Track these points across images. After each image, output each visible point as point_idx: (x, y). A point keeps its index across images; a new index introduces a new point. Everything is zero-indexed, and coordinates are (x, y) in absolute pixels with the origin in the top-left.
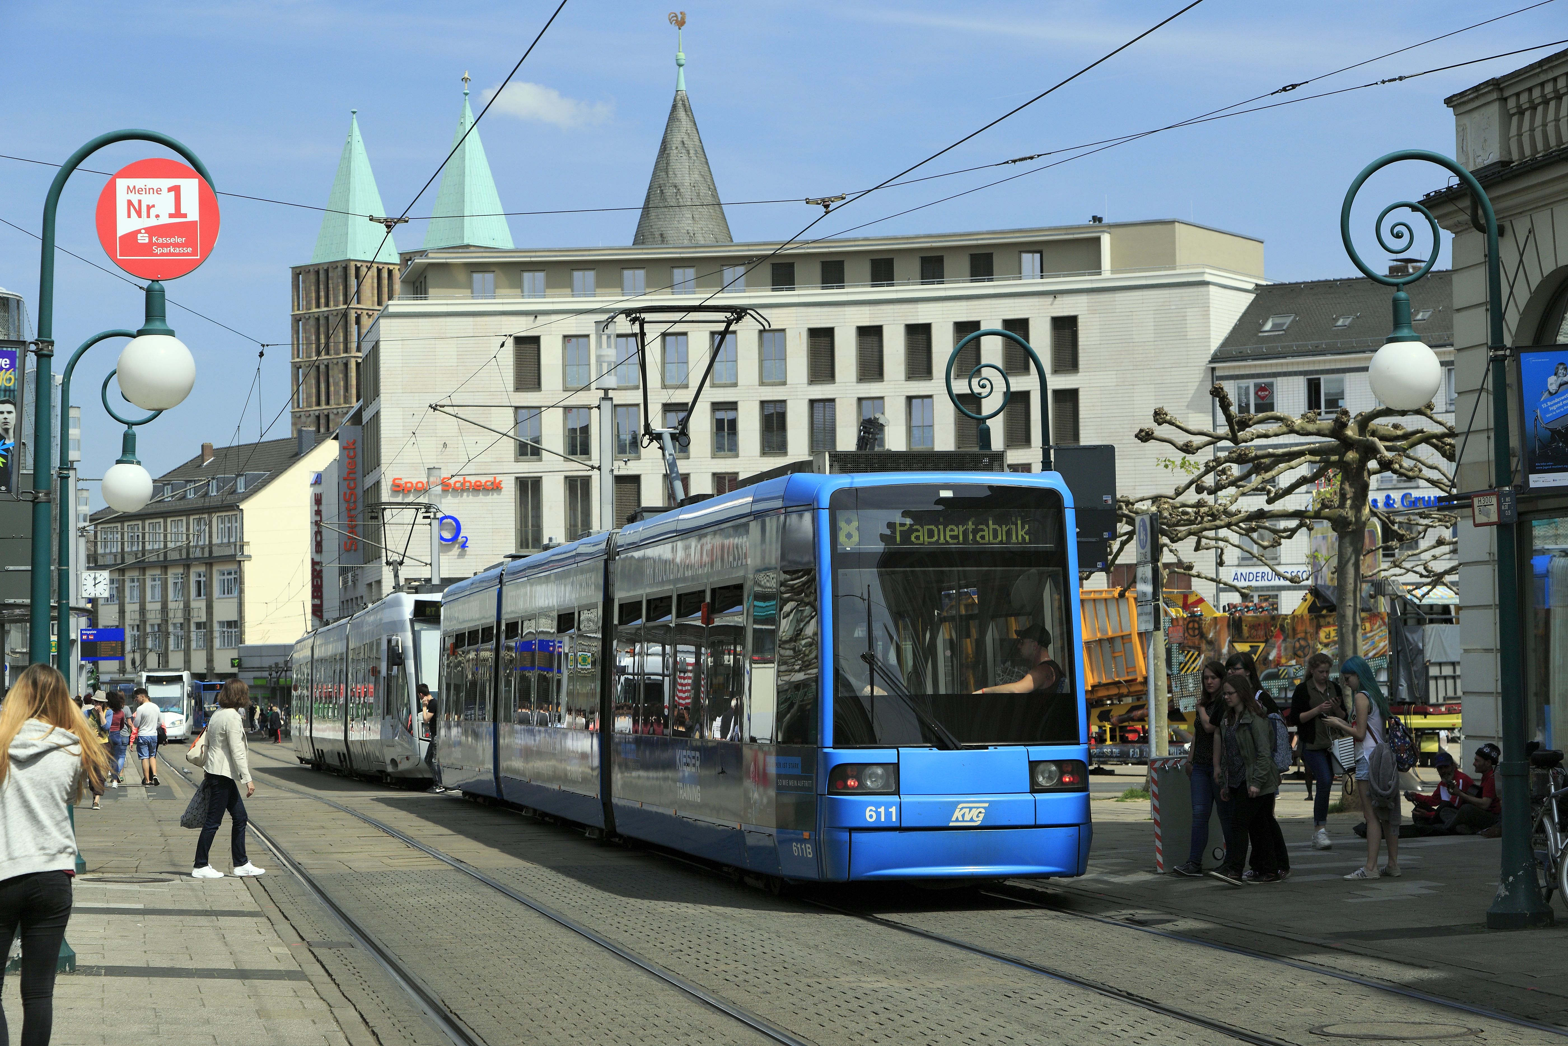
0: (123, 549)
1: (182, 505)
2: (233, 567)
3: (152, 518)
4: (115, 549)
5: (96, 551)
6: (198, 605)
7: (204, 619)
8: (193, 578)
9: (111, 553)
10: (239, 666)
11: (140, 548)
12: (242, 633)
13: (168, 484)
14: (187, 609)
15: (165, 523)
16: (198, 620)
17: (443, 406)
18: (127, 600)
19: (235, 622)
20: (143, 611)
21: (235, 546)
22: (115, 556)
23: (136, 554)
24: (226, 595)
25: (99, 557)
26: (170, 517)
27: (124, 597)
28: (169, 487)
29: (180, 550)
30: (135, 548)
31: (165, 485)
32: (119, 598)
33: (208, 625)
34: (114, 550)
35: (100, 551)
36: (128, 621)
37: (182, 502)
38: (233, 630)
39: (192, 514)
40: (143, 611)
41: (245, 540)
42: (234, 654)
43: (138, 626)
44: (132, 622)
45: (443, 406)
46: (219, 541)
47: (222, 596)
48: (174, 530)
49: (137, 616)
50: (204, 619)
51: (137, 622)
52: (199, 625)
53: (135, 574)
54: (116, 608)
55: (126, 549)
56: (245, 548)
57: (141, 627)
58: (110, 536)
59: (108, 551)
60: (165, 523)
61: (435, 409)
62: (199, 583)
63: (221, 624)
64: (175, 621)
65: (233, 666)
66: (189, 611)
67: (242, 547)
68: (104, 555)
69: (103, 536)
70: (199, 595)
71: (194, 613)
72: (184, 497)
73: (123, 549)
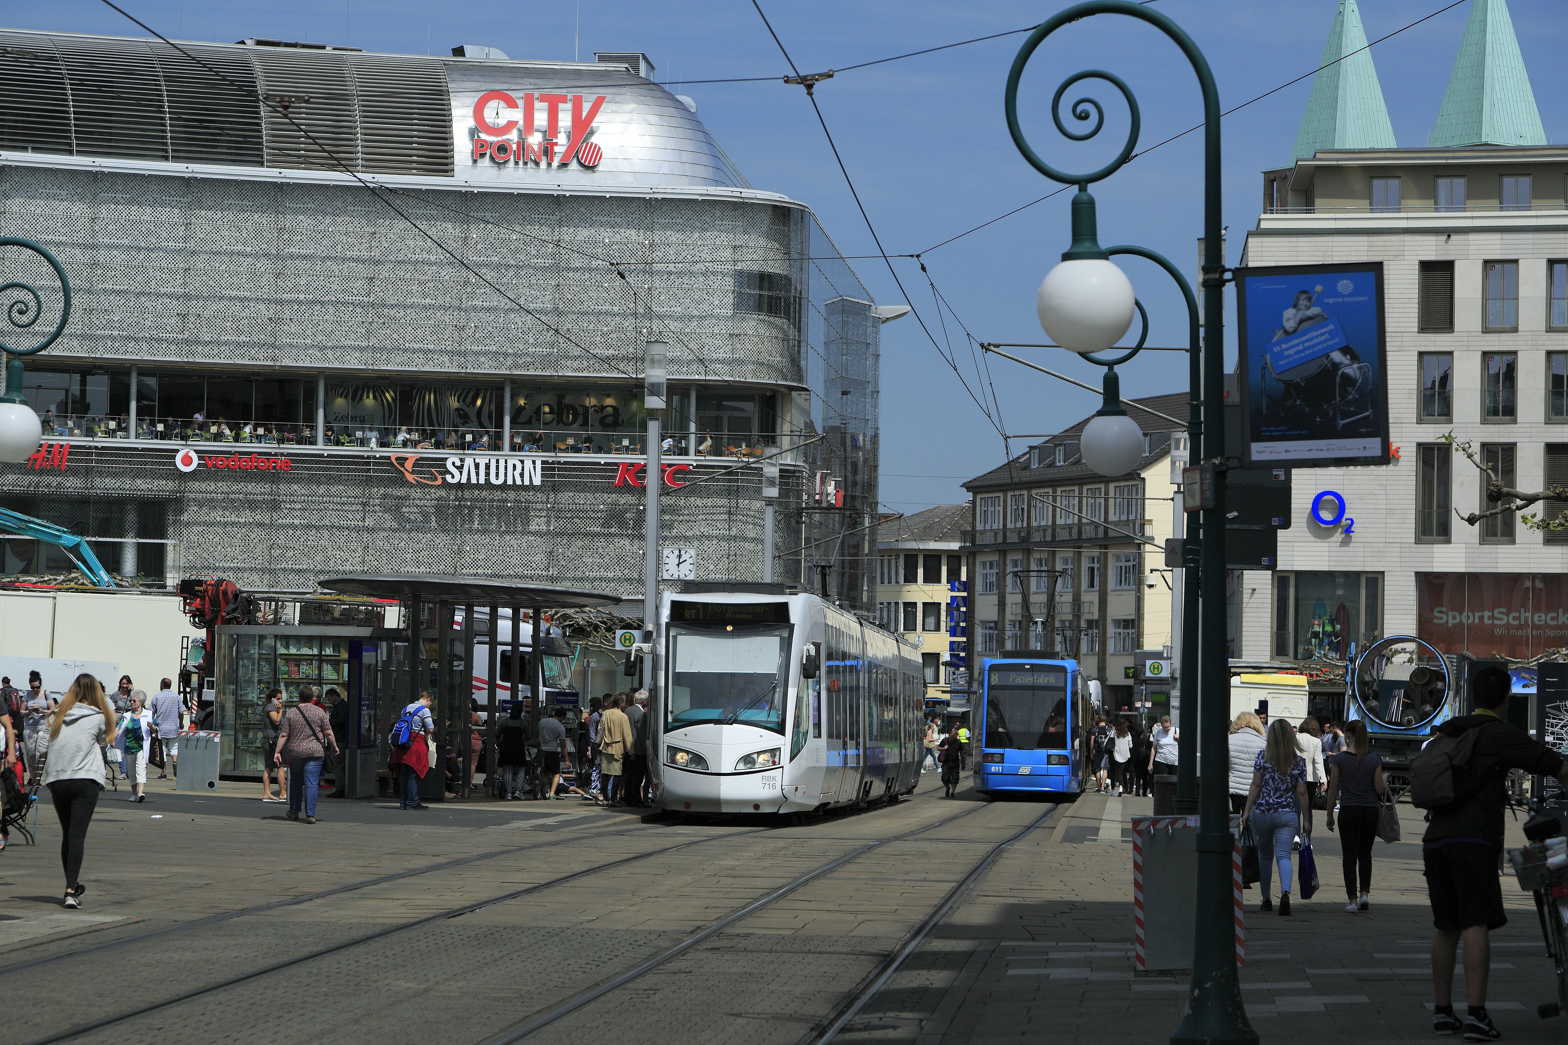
0: (1005, 525)
1: (1051, 474)
2: (1132, 551)
3: (1039, 487)
4: (998, 525)
5: (974, 526)
6: (1090, 598)
7: (1096, 616)
8: (1085, 565)
9: (991, 530)
10: (1135, 676)
11: (1025, 524)
12: (1140, 635)
13: (1060, 445)
14: (1077, 602)
15: (1054, 492)
16: (1089, 617)
17: (998, 346)
18: (1009, 589)
19: (1133, 620)
20: (1026, 603)
21: (1134, 524)
22: (996, 533)
23: (1019, 532)
24: (1123, 587)
25: (978, 535)
26: (1060, 486)
27: (1005, 586)
28: (1062, 448)
29: (1071, 528)
30: (1019, 525)
31: (1057, 445)
32: (998, 586)
33: (1101, 622)
34: (995, 527)
35: (979, 527)
36: (1009, 617)
37: (1075, 468)
38: (1131, 631)
39: (1086, 484)
40: (1026, 603)
41: (1146, 518)
42: (1130, 662)
43: (1020, 622)
44: (1013, 618)
45: (998, 346)
46: (1116, 518)
47: (1118, 587)
48: (1065, 502)
49: (1019, 610)
50: (1096, 616)
51: (1019, 618)
52: (1090, 623)
53: (1019, 556)
54: (994, 599)
55: (1009, 525)
56: (1147, 527)
57: (1024, 624)
58: (991, 509)
59: (988, 527)
60: (1054, 492)
61: (987, 349)
62: (1092, 570)
63: (1117, 623)
64: (1064, 617)
65: (1127, 676)
66: (1079, 605)
67: (1142, 526)
68: (983, 532)
69: (984, 509)
70: (1092, 585)
71: (1085, 609)
72: (1052, 465)
73: (1005, 525)
